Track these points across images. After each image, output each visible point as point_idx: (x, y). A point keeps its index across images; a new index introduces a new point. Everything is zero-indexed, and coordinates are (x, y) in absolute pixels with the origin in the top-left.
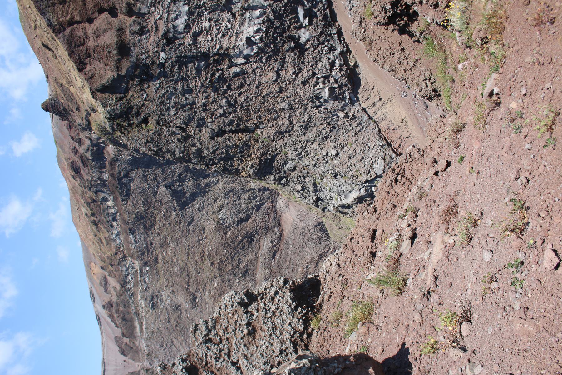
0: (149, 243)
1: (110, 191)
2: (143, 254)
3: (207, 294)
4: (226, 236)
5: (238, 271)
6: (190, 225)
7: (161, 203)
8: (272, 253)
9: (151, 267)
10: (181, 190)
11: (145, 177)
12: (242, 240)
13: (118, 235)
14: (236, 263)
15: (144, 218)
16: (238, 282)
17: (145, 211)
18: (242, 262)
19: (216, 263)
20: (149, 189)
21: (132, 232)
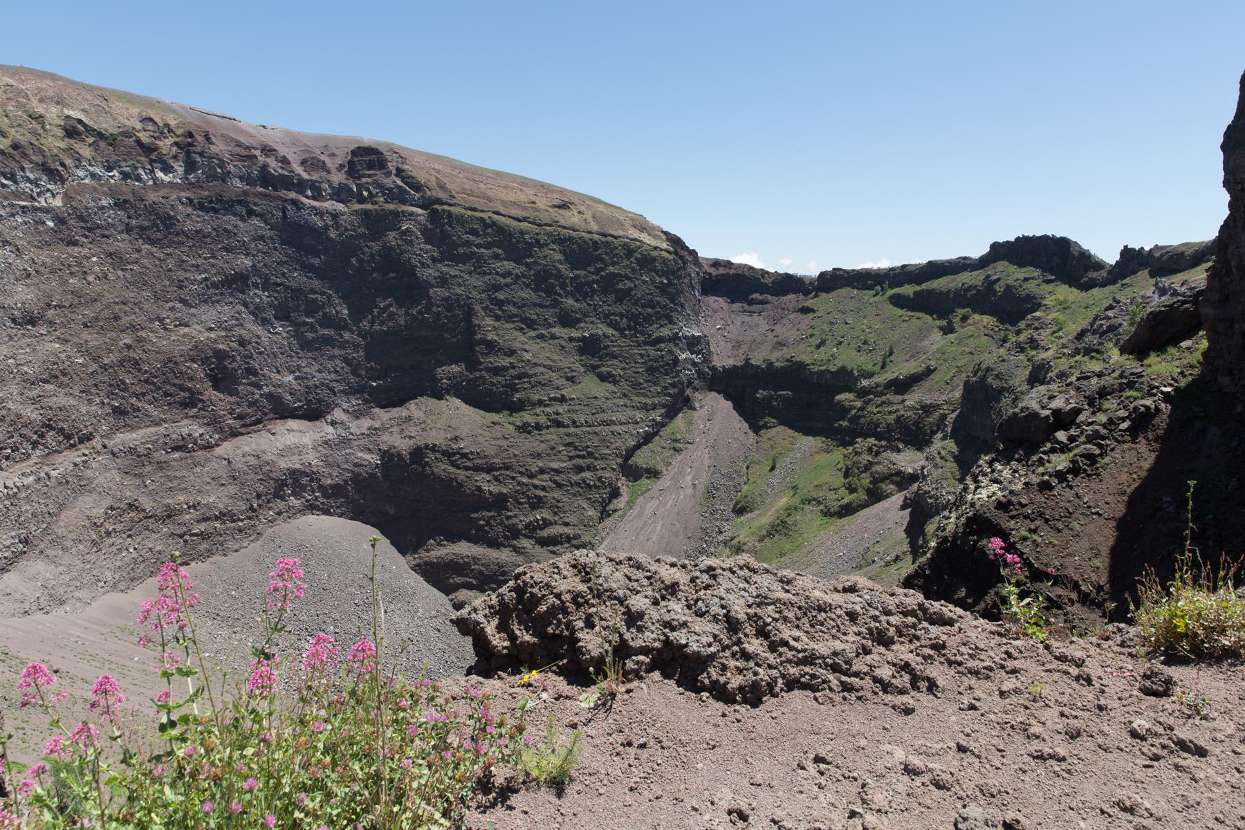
0: (106, 233)
1: (198, 182)
2: (81, 218)
3: (58, 346)
4: (186, 361)
5: (123, 398)
6: (180, 302)
7: (209, 258)
8: (181, 443)
9: (56, 232)
10: (248, 286)
11: (262, 238)
12: (183, 389)
13: (93, 175)
14: (138, 389)
15: (168, 227)
16: (103, 403)
17: (183, 232)
18: (140, 401)
19: (132, 354)
20: (239, 241)
21: (120, 204)
